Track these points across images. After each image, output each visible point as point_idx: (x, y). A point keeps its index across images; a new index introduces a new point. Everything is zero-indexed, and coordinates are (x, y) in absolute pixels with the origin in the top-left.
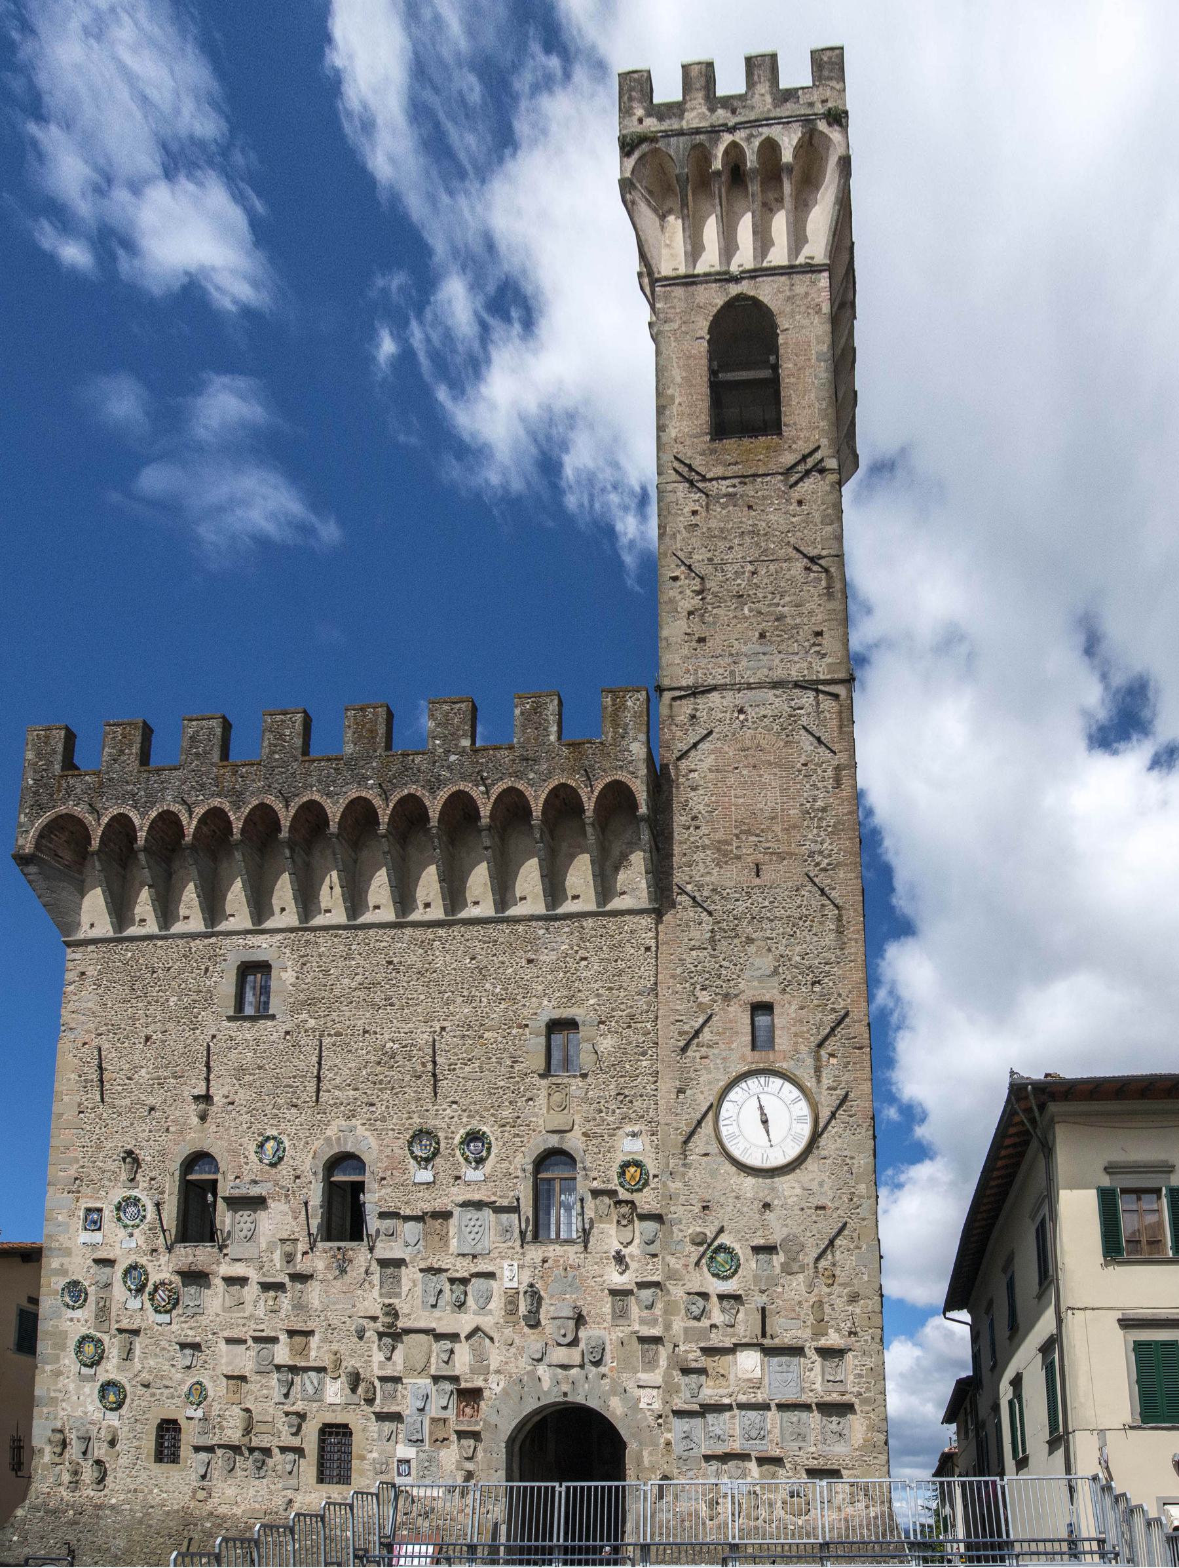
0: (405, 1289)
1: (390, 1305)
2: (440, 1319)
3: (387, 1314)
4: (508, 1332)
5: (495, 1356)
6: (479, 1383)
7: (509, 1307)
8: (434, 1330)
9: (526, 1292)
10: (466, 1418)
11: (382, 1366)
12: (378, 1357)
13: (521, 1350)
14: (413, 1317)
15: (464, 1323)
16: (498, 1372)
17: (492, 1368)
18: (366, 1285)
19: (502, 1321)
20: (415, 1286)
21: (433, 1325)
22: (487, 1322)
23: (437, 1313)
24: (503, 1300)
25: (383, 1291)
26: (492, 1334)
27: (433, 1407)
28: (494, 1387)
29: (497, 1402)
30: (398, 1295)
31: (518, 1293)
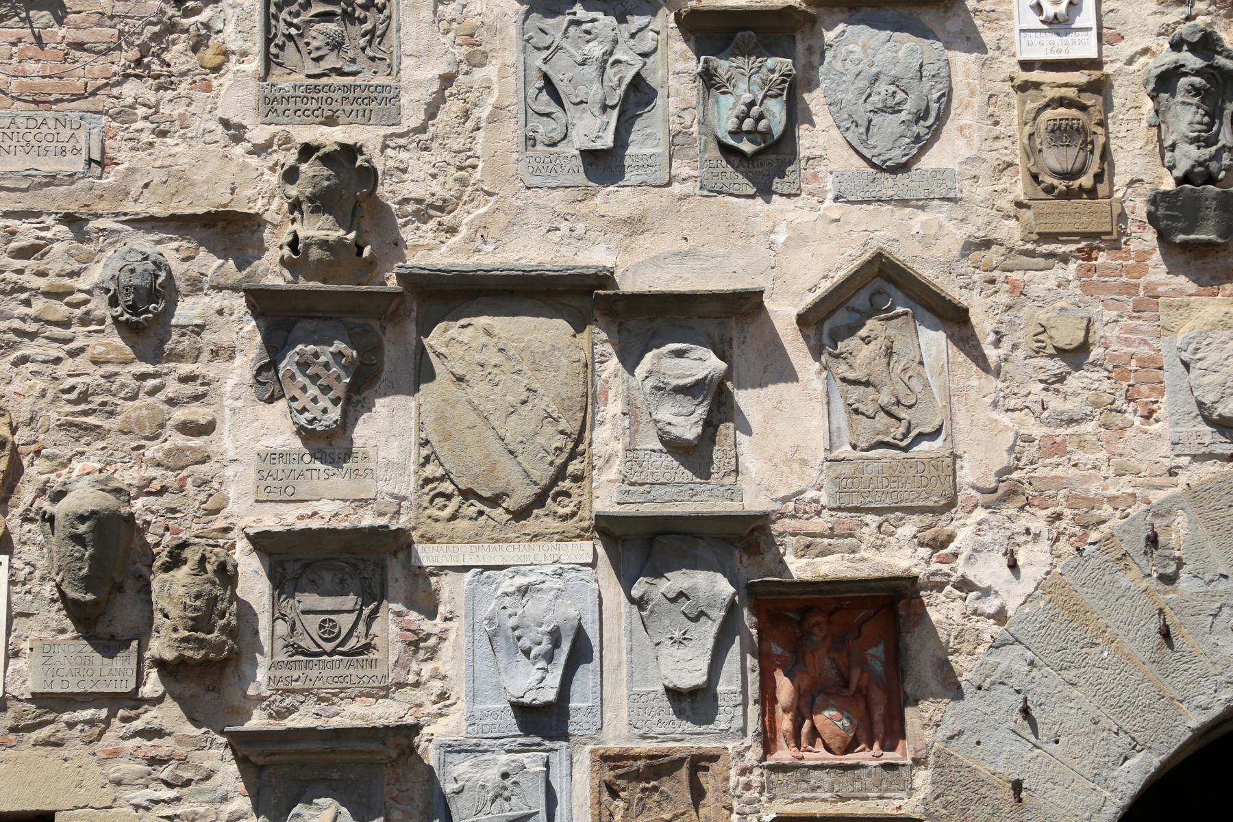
0: (418, 76)
1: (350, 152)
2: (635, 225)
3: (322, 202)
4: (1054, 287)
5: (982, 427)
6: (900, 557)
7: (1055, 158)
8: (605, 279)
9: (1165, 81)
10: (819, 755)
11: (274, 480)
12: (252, 431)
13: (1139, 385)
14: (466, 217)
15: (792, 249)
16: (1005, 492)
17: (968, 474)
18: (178, 54)
19: (1010, 231)
20: (476, 60)
21: (594, 256)
22: (926, 241)
23: (614, 201)
24: (1011, 119)
25: (283, 81)
26: (952, 290)
27: (618, 692)
28: (990, 585)
29: (1012, 660)
30: (380, 103)
31: (1101, 87)
